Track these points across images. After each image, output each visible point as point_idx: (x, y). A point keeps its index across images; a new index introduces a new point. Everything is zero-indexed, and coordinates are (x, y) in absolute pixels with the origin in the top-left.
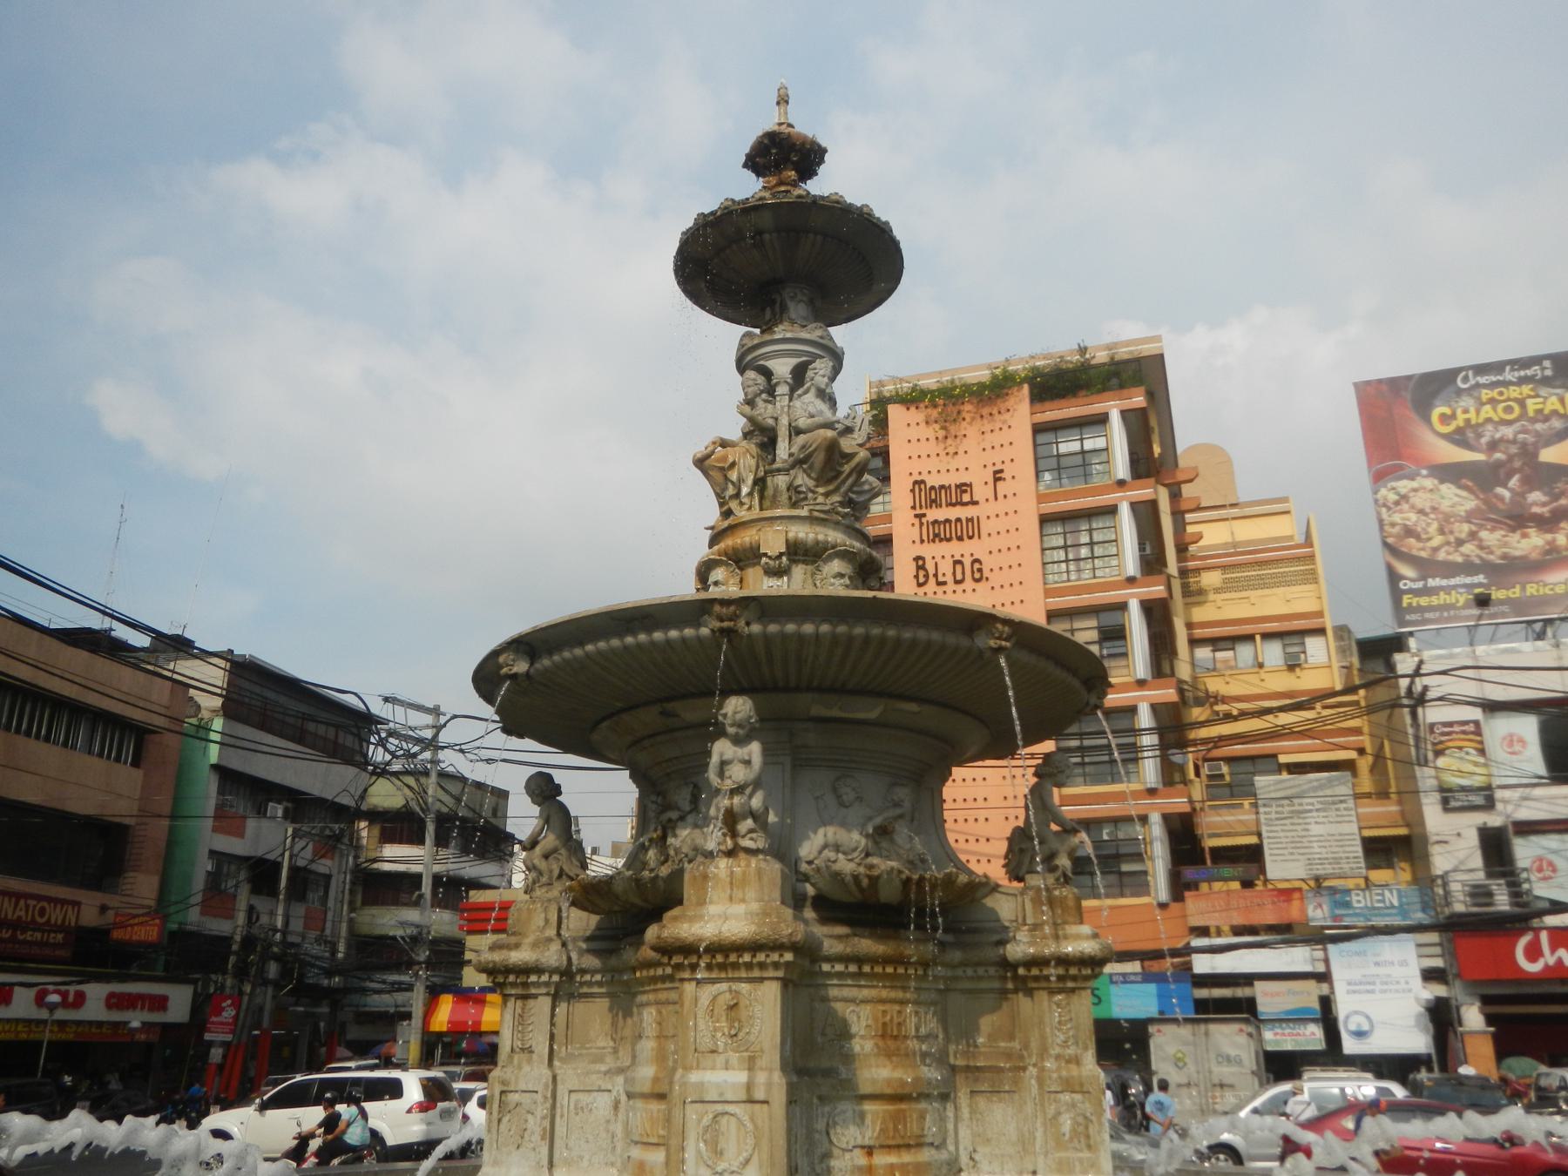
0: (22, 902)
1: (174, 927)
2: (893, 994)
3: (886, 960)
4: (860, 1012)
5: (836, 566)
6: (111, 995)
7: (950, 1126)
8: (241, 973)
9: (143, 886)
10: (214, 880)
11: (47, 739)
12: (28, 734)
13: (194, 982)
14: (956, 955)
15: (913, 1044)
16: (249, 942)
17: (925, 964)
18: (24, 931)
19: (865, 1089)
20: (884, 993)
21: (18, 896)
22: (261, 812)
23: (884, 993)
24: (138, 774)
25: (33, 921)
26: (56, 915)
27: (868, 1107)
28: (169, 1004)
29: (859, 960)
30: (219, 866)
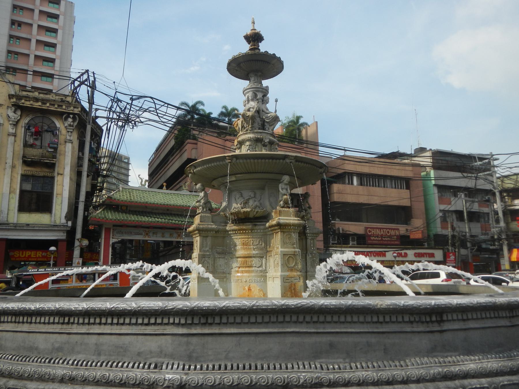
0: (382, 230)
1: (434, 233)
2: (245, 237)
3: (239, 230)
4: (238, 240)
5: (248, 143)
6: (415, 253)
7: (264, 263)
8: (453, 245)
9: (418, 222)
10: (444, 220)
11: (379, 186)
12: (373, 186)
13: (443, 249)
14: (262, 227)
15: (252, 247)
16: (453, 236)
17: (252, 230)
18: (384, 238)
19: (237, 256)
20: (243, 237)
21: (380, 229)
22: (455, 196)
23: (243, 237)
24: (409, 191)
25: (386, 235)
26: (393, 233)
27: (239, 259)
28: (435, 255)
29: (235, 230)
30: (444, 214)
